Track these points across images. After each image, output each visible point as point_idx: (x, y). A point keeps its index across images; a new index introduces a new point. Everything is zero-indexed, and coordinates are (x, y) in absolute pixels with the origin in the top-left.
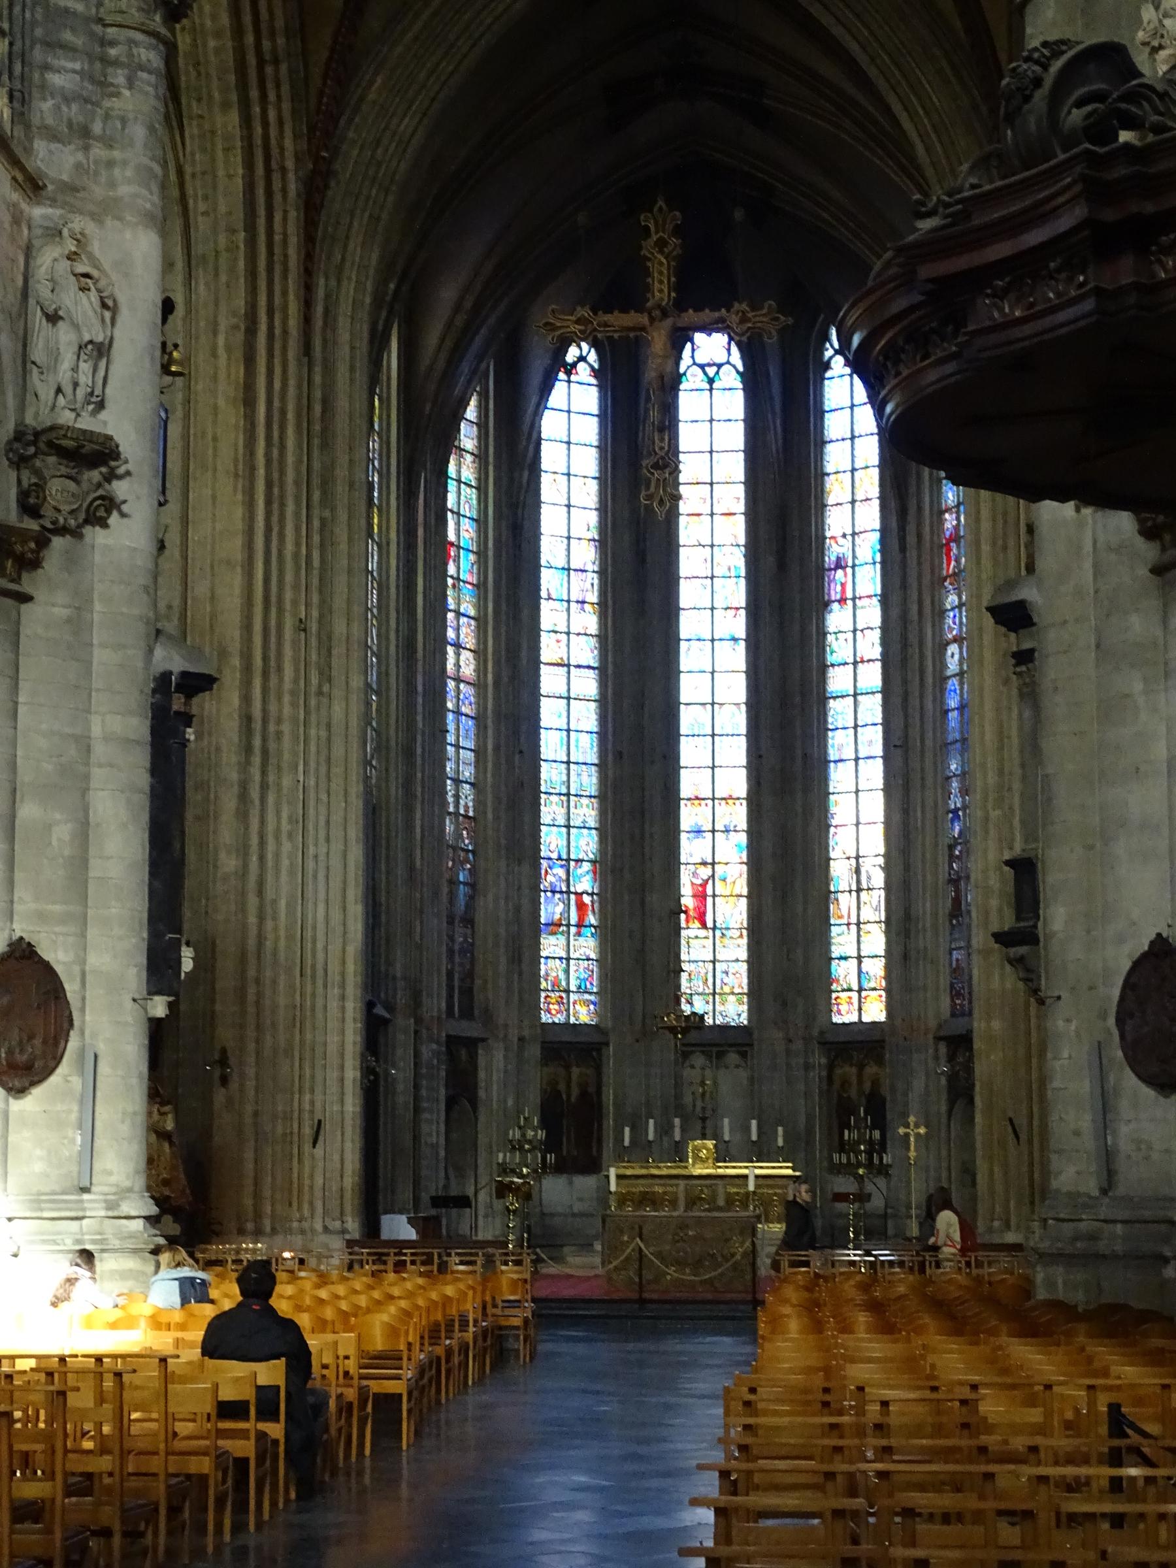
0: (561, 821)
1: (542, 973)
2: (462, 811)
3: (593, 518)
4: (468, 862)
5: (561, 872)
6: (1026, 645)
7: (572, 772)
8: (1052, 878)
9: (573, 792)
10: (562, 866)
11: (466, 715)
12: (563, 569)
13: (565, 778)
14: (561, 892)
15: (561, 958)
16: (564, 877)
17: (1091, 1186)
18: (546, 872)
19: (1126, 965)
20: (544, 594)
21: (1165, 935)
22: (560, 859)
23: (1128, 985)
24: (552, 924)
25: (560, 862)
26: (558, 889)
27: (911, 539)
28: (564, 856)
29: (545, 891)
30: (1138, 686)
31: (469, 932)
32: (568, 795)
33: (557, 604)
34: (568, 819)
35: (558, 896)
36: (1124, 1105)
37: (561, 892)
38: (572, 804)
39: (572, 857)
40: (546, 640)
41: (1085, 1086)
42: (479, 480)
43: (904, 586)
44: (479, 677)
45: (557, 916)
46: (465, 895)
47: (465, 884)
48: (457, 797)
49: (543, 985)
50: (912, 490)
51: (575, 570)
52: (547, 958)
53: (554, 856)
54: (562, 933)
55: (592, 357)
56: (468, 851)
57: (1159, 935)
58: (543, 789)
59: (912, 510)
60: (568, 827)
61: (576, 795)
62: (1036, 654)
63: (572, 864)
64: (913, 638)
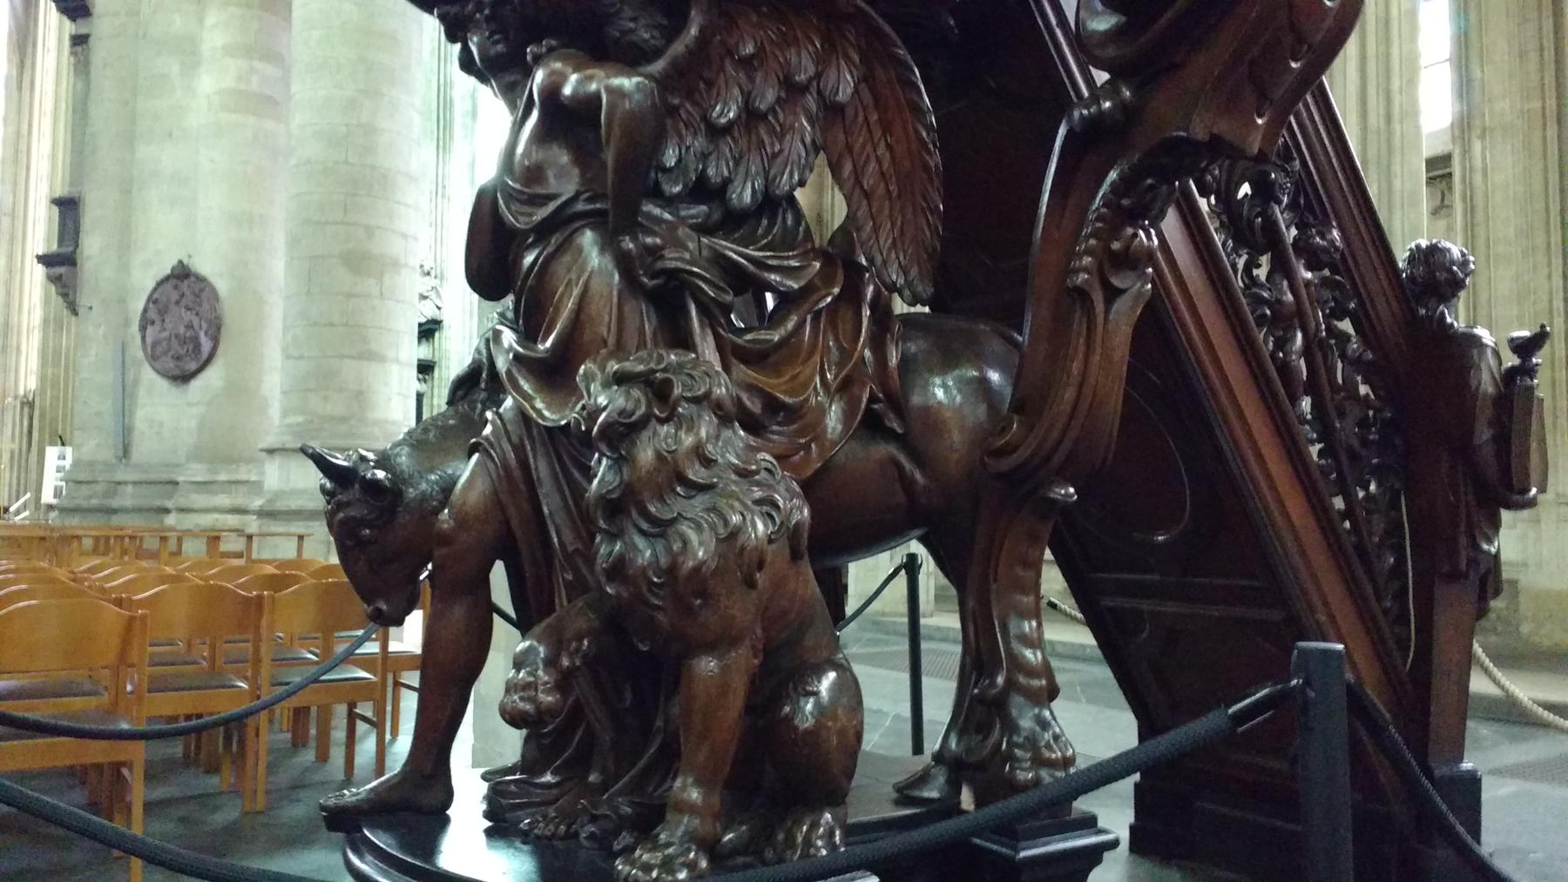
6: (84, 31)
8: (91, 215)
17: (107, 454)
19: (151, 285)
21: (185, 262)
23: (151, 299)
27: (26, 84)
30: (175, 69)
36: (142, 392)
41: (108, 377)
43: (19, 112)
50: (30, 50)
57: (180, 262)
59: (28, 63)
62: (91, 39)
64: (23, 147)
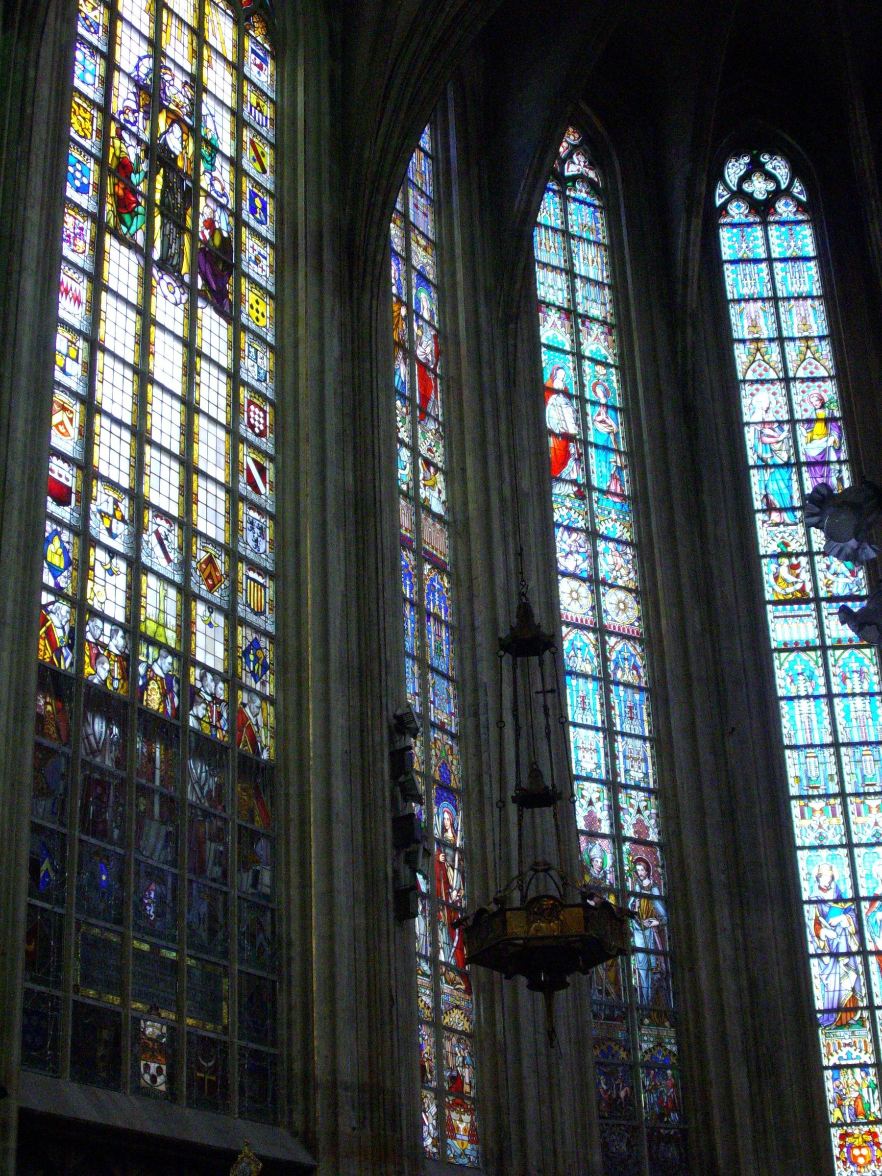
0: (835, 837)
1: (830, 1095)
2: (629, 831)
3: (830, 390)
4: (652, 914)
5: (846, 922)
7: (845, 759)
9: (849, 789)
10: (846, 911)
11: (627, 685)
12: (787, 465)
13: (833, 769)
14: (849, 954)
15: (863, 1066)
16: (852, 929)
18: (818, 924)
20: (758, 505)
22: (839, 899)
24: (839, 1009)
25: (841, 905)
26: (843, 949)
28: (849, 894)
29: (819, 956)
31: (668, 1033)
32: (842, 795)
33: (787, 517)
34: (848, 833)
35: (843, 961)
37: (849, 954)
38: (851, 808)
39: (863, 893)
40: (768, 568)
42: (621, 356)
44: (647, 628)
45: (846, 996)
46: (649, 969)
47: (646, 951)
48: (615, 810)
49: (835, 1115)
51: (809, 464)
52: (837, 1067)
53: (830, 895)
54: (861, 1022)
55: (797, 188)
56: (650, 897)
58: (793, 791)
60: (850, 846)
61: (857, 795)
63: (865, 905)
